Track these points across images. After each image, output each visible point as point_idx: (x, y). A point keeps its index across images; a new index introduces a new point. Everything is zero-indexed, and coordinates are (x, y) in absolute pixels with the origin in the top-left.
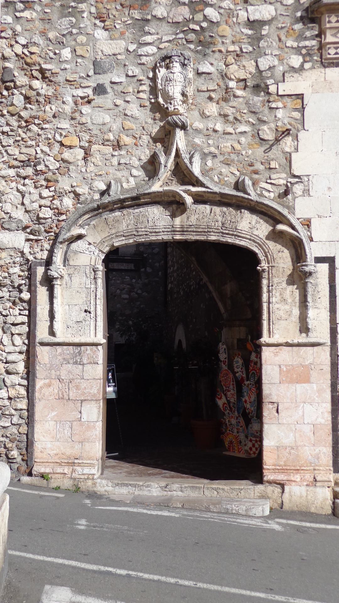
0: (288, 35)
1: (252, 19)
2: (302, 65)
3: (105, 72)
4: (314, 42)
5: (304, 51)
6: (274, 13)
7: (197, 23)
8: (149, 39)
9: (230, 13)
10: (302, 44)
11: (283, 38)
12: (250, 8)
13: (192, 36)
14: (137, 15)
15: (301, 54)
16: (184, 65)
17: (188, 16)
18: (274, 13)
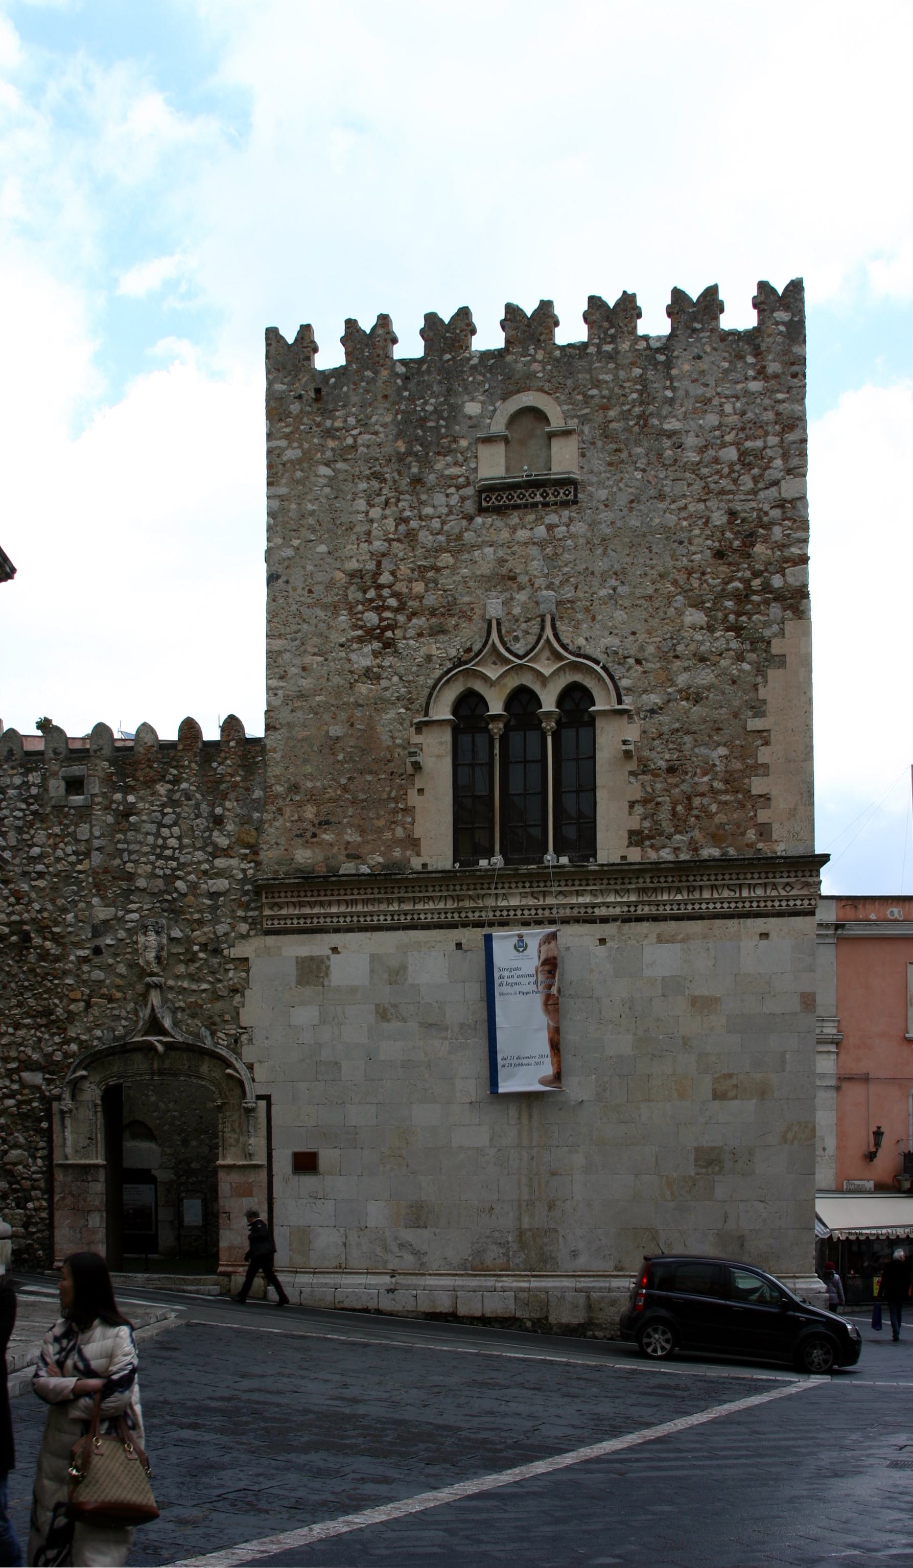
0: (239, 906)
1: (212, 890)
2: (248, 933)
3: (100, 936)
4: (256, 913)
5: (250, 920)
6: (228, 886)
7: (170, 894)
8: (133, 906)
9: (194, 886)
10: (250, 914)
11: (235, 908)
12: (210, 882)
13: (166, 905)
14: (124, 885)
15: (247, 923)
16: (158, 933)
17: (163, 888)
18: (228, 886)
